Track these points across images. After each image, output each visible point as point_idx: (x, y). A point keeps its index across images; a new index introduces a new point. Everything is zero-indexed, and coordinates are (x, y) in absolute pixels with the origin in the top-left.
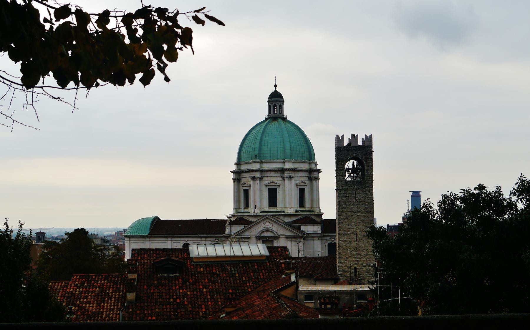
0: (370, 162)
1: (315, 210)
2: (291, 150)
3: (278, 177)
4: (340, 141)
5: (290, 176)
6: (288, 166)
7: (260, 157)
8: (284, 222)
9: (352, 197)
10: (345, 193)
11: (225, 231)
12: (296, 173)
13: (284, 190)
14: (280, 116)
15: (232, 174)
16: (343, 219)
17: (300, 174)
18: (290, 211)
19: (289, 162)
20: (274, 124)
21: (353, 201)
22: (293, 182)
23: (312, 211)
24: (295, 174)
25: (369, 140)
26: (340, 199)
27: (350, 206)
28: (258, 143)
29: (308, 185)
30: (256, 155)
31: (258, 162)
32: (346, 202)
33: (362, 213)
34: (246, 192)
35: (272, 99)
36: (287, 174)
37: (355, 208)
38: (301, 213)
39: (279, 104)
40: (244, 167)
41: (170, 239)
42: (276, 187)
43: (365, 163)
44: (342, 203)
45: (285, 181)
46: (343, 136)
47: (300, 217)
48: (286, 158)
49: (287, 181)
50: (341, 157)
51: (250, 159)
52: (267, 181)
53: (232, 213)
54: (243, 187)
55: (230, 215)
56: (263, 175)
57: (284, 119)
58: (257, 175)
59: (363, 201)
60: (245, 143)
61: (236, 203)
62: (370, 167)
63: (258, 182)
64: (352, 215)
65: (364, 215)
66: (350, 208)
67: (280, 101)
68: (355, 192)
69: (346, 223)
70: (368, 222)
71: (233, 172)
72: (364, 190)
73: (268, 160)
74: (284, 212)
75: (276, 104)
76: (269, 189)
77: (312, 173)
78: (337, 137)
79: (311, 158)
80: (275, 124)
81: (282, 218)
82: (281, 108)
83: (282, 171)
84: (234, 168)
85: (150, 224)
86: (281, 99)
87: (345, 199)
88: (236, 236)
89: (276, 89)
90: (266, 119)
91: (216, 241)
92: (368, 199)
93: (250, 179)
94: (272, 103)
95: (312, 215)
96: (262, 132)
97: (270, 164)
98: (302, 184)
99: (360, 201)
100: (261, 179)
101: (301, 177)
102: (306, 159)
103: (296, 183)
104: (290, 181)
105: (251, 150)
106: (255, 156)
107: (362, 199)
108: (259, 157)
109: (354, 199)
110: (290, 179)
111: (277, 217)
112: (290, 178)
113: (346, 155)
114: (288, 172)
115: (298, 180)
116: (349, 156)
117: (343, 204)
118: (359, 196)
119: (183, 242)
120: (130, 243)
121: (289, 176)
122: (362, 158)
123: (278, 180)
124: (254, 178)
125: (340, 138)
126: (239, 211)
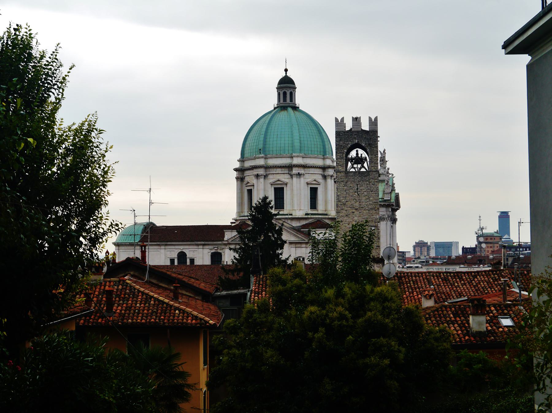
0: (375, 149)
1: (329, 213)
2: (301, 144)
3: (285, 174)
4: (339, 125)
5: (299, 173)
6: (296, 161)
7: (264, 152)
8: (292, 227)
9: (353, 191)
10: (345, 185)
12: (306, 169)
13: (292, 190)
14: (291, 105)
16: (342, 216)
17: (312, 171)
20: (284, 114)
21: (354, 195)
22: (303, 180)
23: (326, 215)
24: (305, 171)
25: (374, 123)
26: (339, 193)
27: (350, 201)
28: (263, 136)
29: (321, 184)
30: (260, 149)
31: (262, 158)
32: (346, 197)
33: (365, 209)
34: (250, 192)
35: (282, 85)
36: (295, 171)
37: (357, 204)
38: (312, 216)
39: (290, 91)
40: (248, 164)
41: (163, 247)
42: (283, 187)
43: (368, 150)
44: (341, 199)
45: (293, 179)
46: (343, 119)
47: (310, 220)
48: (295, 153)
49: (295, 179)
50: (341, 144)
51: (254, 153)
52: (272, 179)
54: (246, 186)
56: (268, 173)
57: (295, 108)
58: (261, 172)
59: (366, 195)
60: (250, 136)
61: (239, 205)
62: (375, 155)
63: (262, 180)
64: (353, 212)
65: (367, 211)
66: (350, 204)
67: (290, 88)
68: (357, 185)
69: (346, 221)
70: (372, 221)
71: (236, 170)
72: (367, 182)
73: (274, 155)
74: (291, 215)
75: (286, 91)
76: (274, 188)
77: (327, 170)
78: (336, 120)
79: (326, 153)
80: (284, 113)
81: (289, 222)
83: (290, 167)
84: (237, 165)
85: (141, 229)
86: (292, 85)
87: (345, 193)
88: (231, 241)
89: (286, 73)
90: (275, 108)
91: (215, 250)
92: (373, 193)
93: (253, 178)
94: (281, 89)
95: (325, 218)
96: (268, 123)
97: (276, 159)
98: (315, 182)
99: (363, 195)
100: (266, 177)
101: (312, 174)
102: (319, 153)
103: (307, 181)
104: (298, 179)
105: (255, 144)
106: (259, 150)
107: (365, 193)
108: (264, 151)
109: (356, 193)
110: (298, 176)
111: (283, 220)
112: (299, 175)
113: (347, 142)
114: (297, 169)
116: (350, 143)
117: (342, 200)
118: (361, 190)
119: (178, 250)
120: (119, 251)
121: (297, 173)
122: (366, 144)
123: (285, 178)
124: (257, 176)
125: (340, 121)
126: (242, 215)
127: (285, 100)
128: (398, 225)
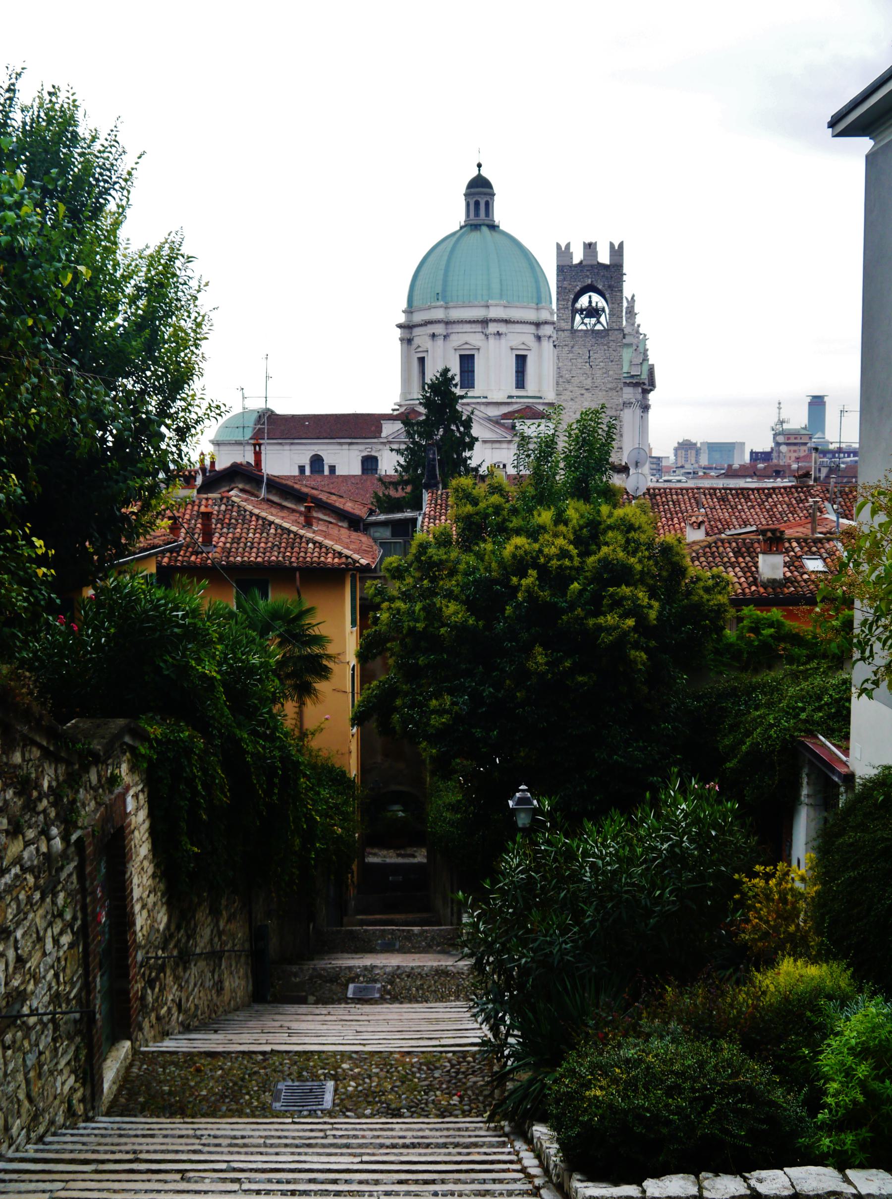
1: (543, 395)
2: (501, 285)
6: (493, 313)
7: (444, 298)
10: (570, 352)
11: (381, 431)
12: (510, 326)
14: (486, 222)
15: (399, 330)
16: (566, 401)
18: (501, 397)
19: (496, 306)
20: (475, 236)
22: (505, 343)
23: (541, 398)
25: (617, 252)
28: (442, 272)
34: (422, 360)
35: (473, 190)
36: (492, 328)
38: (518, 400)
40: (418, 318)
41: (287, 447)
46: (568, 245)
49: (492, 340)
52: (456, 340)
53: (398, 400)
55: (395, 404)
56: (450, 331)
57: (493, 227)
58: (439, 329)
60: (422, 273)
64: (582, 395)
65: (604, 393)
67: (485, 194)
71: (400, 326)
77: (542, 327)
78: (558, 246)
81: (482, 408)
82: (488, 206)
83: (485, 322)
84: (402, 319)
86: (487, 190)
90: (461, 228)
95: (539, 403)
97: (462, 309)
100: (446, 337)
108: (443, 297)
110: (497, 337)
123: (476, 339)
127: (477, 214)
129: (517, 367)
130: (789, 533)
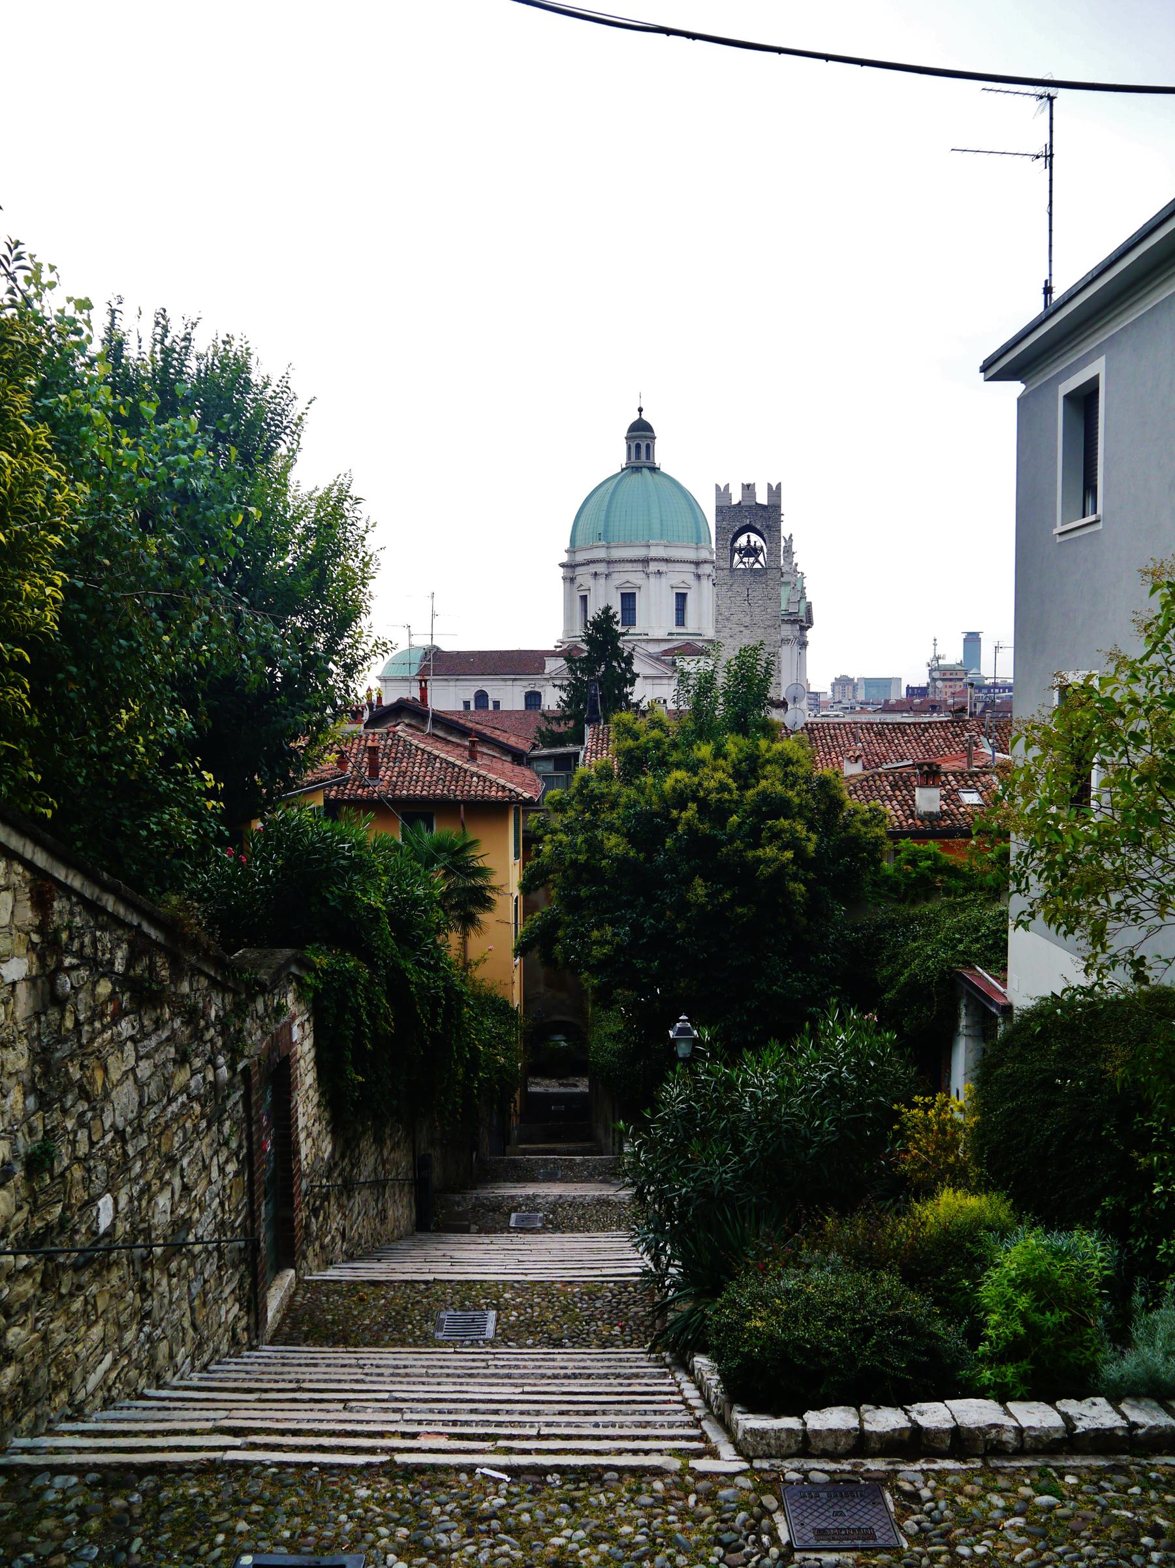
6: (654, 552)
10: (729, 590)
12: (670, 565)
15: (562, 569)
17: (678, 567)
18: (662, 634)
20: (636, 477)
22: (665, 582)
25: (775, 492)
34: (584, 599)
36: (653, 567)
40: (581, 557)
49: (652, 579)
52: (617, 579)
53: (561, 637)
57: (654, 469)
58: (601, 568)
63: (602, 581)
71: (562, 565)
81: (643, 645)
82: (649, 449)
83: (646, 561)
84: (565, 558)
86: (648, 434)
90: (623, 470)
93: (589, 577)
104: (658, 580)
108: (604, 537)
114: (656, 563)
115: (675, 579)
123: (637, 578)
127: (638, 457)
128: (809, 649)
129: (677, 605)
130: (945, 767)
